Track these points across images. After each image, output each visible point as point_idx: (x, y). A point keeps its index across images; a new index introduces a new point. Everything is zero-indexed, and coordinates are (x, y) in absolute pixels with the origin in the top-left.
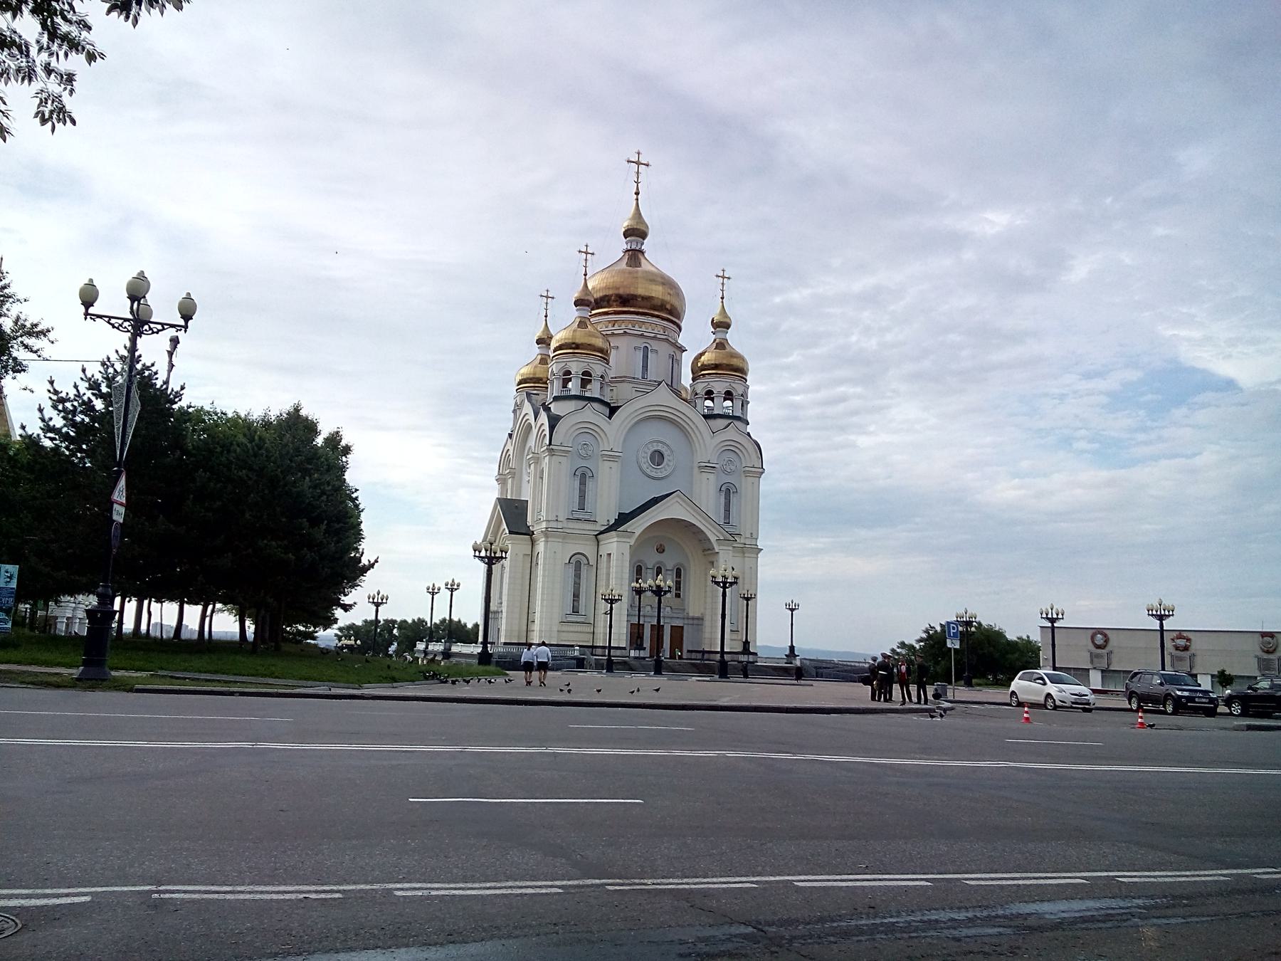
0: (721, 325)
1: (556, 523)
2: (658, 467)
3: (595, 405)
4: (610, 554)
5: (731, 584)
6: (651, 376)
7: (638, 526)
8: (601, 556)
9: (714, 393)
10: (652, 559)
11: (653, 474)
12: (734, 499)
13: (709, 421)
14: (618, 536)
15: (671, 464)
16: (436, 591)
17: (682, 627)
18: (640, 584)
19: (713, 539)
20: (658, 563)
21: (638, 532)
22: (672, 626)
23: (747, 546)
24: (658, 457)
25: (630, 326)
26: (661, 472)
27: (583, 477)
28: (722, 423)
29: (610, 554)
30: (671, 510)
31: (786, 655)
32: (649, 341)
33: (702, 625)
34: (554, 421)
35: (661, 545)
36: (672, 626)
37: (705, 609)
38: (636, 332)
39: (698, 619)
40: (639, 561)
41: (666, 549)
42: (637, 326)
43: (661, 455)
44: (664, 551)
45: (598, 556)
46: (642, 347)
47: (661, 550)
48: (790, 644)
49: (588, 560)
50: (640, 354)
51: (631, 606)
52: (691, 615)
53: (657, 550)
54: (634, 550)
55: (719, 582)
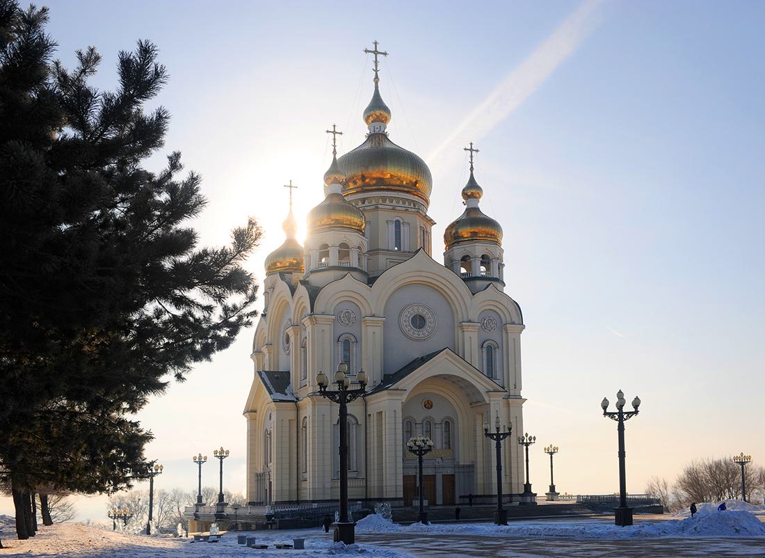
0: (472, 191)
3: (355, 274)
4: (382, 412)
6: (406, 245)
7: (410, 382)
8: (370, 415)
10: (420, 414)
12: (497, 355)
13: (469, 283)
14: (389, 394)
17: (454, 475)
21: (410, 388)
24: (419, 321)
25: (381, 202)
28: (479, 283)
29: (382, 412)
30: (442, 365)
32: (400, 215)
33: (473, 472)
34: (314, 294)
35: (428, 401)
36: (443, 475)
37: (476, 457)
38: (387, 207)
39: (469, 466)
41: (434, 404)
44: (432, 406)
45: (367, 416)
47: (428, 405)
49: (356, 420)
50: (392, 227)
52: (461, 463)
53: (425, 406)
54: (405, 407)
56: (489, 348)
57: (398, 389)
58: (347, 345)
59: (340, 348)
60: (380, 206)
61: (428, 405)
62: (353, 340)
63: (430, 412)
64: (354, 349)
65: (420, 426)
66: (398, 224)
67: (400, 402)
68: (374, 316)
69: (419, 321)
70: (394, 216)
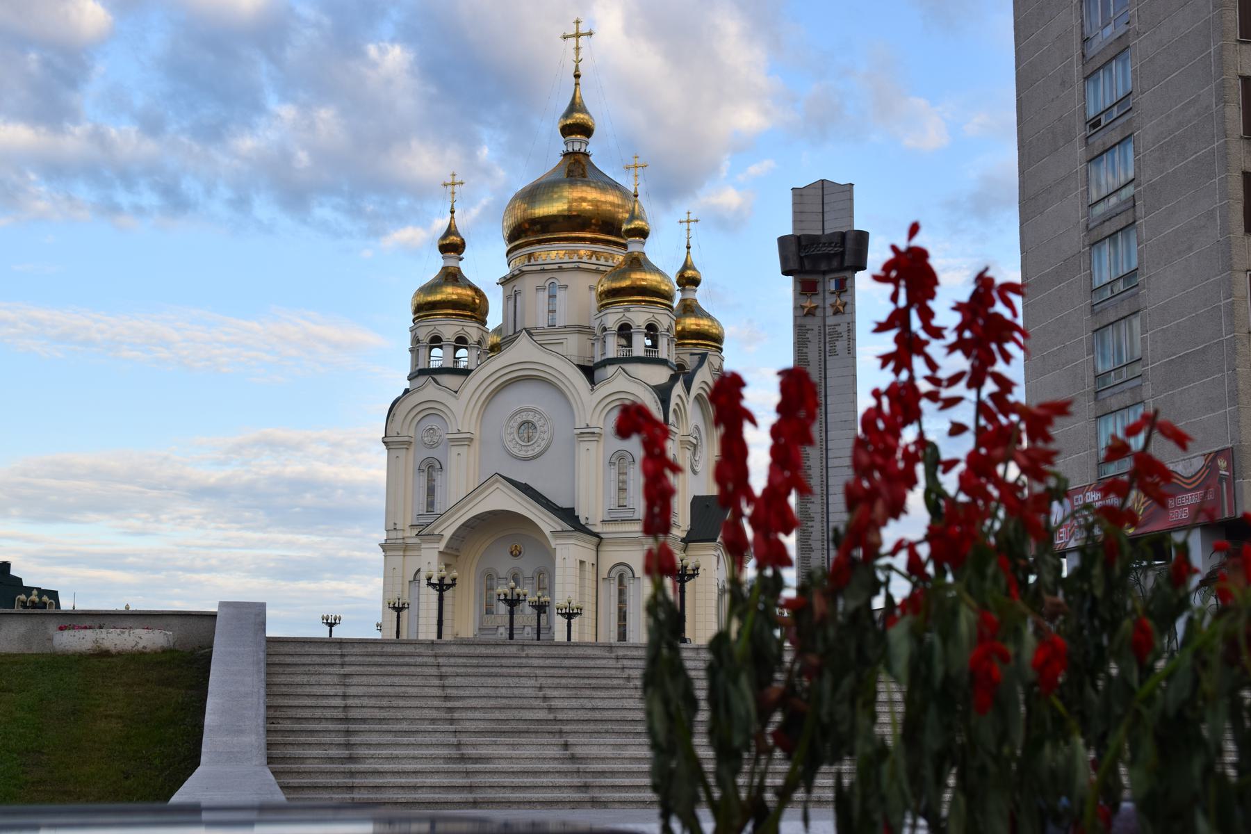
1: (395, 532)
2: (529, 444)
5: (449, 586)
9: (632, 328)
11: (530, 453)
15: (545, 436)
19: (546, 529)
21: (448, 534)
26: (539, 446)
27: (431, 468)
32: (555, 275)
41: (523, 551)
44: (520, 553)
46: (547, 285)
50: (544, 296)
51: (480, 629)
53: (512, 553)
55: (436, 584)
62: (439, 467)
64: (439, 478)
67: (437, 550)
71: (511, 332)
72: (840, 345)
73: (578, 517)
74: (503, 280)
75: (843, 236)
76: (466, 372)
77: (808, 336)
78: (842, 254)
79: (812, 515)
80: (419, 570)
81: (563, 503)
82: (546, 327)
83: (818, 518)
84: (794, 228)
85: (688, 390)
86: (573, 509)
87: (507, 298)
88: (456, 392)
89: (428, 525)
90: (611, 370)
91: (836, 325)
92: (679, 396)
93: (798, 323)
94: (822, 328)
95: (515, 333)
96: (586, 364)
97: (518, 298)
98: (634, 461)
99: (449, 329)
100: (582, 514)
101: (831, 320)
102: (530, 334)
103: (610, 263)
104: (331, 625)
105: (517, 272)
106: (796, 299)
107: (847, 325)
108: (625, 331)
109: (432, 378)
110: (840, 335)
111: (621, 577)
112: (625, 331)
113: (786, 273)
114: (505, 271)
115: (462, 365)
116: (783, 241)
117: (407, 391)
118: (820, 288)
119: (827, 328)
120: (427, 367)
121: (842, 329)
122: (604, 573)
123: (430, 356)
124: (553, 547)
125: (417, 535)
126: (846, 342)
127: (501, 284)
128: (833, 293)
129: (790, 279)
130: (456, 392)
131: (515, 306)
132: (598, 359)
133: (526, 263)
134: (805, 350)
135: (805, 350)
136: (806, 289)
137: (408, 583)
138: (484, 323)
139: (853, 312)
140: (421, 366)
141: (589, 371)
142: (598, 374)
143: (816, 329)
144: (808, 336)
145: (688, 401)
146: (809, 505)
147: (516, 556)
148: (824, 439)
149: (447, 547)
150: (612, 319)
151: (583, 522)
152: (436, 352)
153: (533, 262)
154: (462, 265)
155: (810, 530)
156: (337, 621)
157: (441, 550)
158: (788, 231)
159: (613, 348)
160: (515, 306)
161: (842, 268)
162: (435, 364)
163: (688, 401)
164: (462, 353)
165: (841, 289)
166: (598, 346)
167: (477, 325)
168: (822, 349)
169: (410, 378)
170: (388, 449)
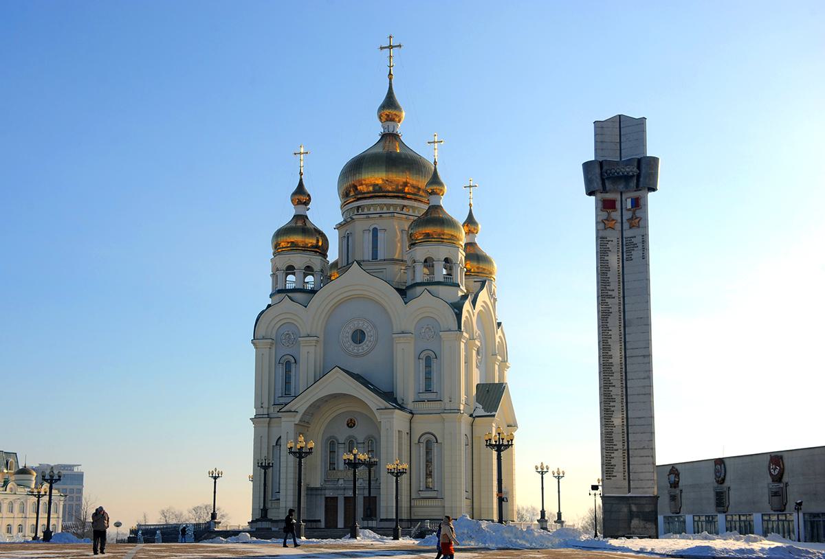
12: (435, 366)
16: (561, 475)
18: (355, 455)
20: (350, 437)
21: (302, 410)
22: (326, 498)
23: (445, 411)
24: (359, 336)
31: (100, 515)
35: (351, 420)
40: (331, 437)
42: (366, 211)
43: (363, 333)
44: (354, 425)
46: (371, 229)
47: (351, 424)
48: (541, 509)
53: (348, 425)
56: (428, 359)
57: (290, 411)
58: (288, 364)
59: (281, 371)
60: (354, 217)
61: (351, 424)
62: (293, 361)
63: (350, 432)
65: (343, 446)
66: (375, 231)
68: (308, 336)
69: (359, 336)
70: (371, 224)
71: (345, 264)
72: (636, 254)
73: (396, 398)
74: (339, 226)
75: (639, 161)
76: (313, 292)
77: (608, 246)
78: (639, 176)
79: (614, 397)
80: (280, 437)
81: (384, 388)
82: (370, 259)
83: (618, 399)
84: (596, 156)
85: (474, 306)
86: (393, 392)
87: (341, 238)
88: (306, 307)
89: (286, 405)
90: (419, 289)
91: (632, 237)
92: (484, 302)
93: (600, 236)
94: (620, 240)
95: (348, 265)
96: (400, 287)
97: (350, 239)
98: (436, 358)
99: (299, 260)
100: (399, 395)
101: (627, 233)
102: (359, 264)
103: (416, 214)
104: (215, 478)
105: (349, 220)
106: (597, 216)
107: (641, 237)
108: (428, 263)
109: (288, 296)
110: (635, 245)
111: (428, 442)
112: (428, 263)
113: (590, 193)
114: (341, 219)
115: (309, 287)
116: (587, 166)
117: (269, 306)
118: (618, 205)
119: (624, 239)
120: (284, 288)
121: (637, 240)
122: (415, 440)
123: (286, 281)
124: (379, 421)
125: (278, 412)
126: (641, 252)
127: (337, 229)
128: (629, 210)
129: (593, 198)
130: (306, 307)
131: (348, 245)
132: (409, 283)
133: (356, 213)
134: (606, 258)
135: (606, 258)
136: (606, 206)
137: (271, 447)
138: (325, 256)
139: (646, 227)
140: (280, 287)
141: (404, 292)
142: (409, 293)
143: (615, 240)
144: (608, 246)
145: (474, 315)
146: (611, 388)
147: (351, 427)
148: (623, 333)
149: (300, 421)
150: (421, 252)
151: (400, 402)
152: (291, 278)
153: (360, 211)
154: (308, 213)
155: (613, 409)
156: (220, 475)
157: (296, 423)
158: (591, 157)
159: (421, 274)
160: (348, 245)
161: (638, 188)
162: (289, 286)
163: (474, 315)
164: (310, 279)
165: (636, 207)
166: (410, 272)
167: (320, 257)
168: (621, 257)
169: (271, 296)
170: (256, 348)
